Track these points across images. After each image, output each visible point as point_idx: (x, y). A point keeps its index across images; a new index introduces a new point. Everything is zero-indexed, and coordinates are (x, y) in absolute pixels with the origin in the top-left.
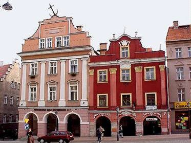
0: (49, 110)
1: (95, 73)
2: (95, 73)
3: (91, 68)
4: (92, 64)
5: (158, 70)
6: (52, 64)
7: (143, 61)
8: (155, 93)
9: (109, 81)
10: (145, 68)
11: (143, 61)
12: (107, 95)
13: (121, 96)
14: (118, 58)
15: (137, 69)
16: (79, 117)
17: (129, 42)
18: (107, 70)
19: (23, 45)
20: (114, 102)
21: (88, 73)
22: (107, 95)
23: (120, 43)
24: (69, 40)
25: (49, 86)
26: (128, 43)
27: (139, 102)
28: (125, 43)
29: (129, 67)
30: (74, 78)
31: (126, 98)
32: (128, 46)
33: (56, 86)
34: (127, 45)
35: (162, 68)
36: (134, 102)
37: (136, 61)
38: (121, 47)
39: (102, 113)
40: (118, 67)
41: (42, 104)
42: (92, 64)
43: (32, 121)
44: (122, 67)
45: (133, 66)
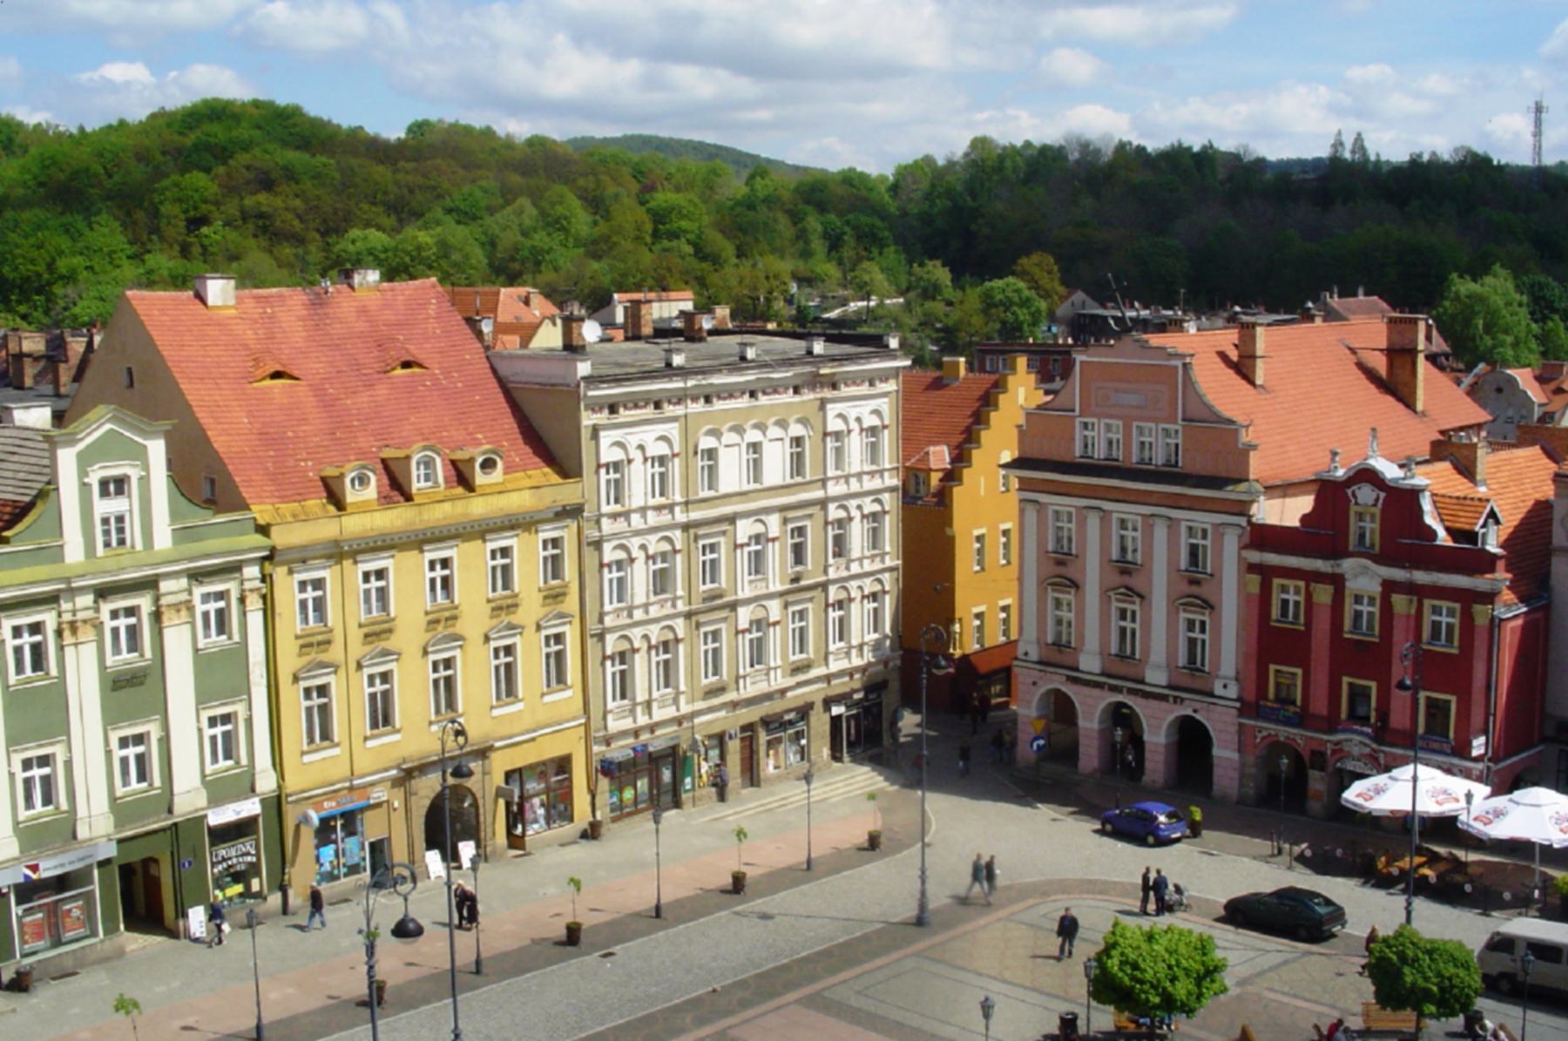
0: (1114, 689)
1: (1266, 588)
2: (1266, 588)
3: (1252, 568)
4: (1255, 556)
5: (1467, 619)
6: (1123, 524)
7: (1421, 577)
8: (1453, 699)
9: (1308, 623)
10: (1427, 603)
11: (1421, 577)
12: (1299, 671)
13: (1345, 688)
14: (1337, 550)
15: (1400, 602)
16: (1210, 728)
17: (1382, 495)
18: (1302, 584)
19: (1019, 427)
20: (1320, 706)
21: (1242, 584)
22: (1299, 671)
23: (1349, 492)
24: (1180, 441)
25: (1115, 604)
26: (1377, 500)
27: (1399, 719)
28: (1366, 494)
29: (1376, 589)
30: (1194, 589)
31: (1358, 695)
32: (1377, 511)
33: (1137, 607)
34: (1375, 505)
35: (1481, 612)
36: (1383, 714)
37: (1398, 574)
38: (1353, 509)
39: (1283, 732)
40: (1338, 581)
41: (1090, 663)
42: (1255, 556)
43: (1061, 710)
44: (1353, 585)
45: (1389, 587)
